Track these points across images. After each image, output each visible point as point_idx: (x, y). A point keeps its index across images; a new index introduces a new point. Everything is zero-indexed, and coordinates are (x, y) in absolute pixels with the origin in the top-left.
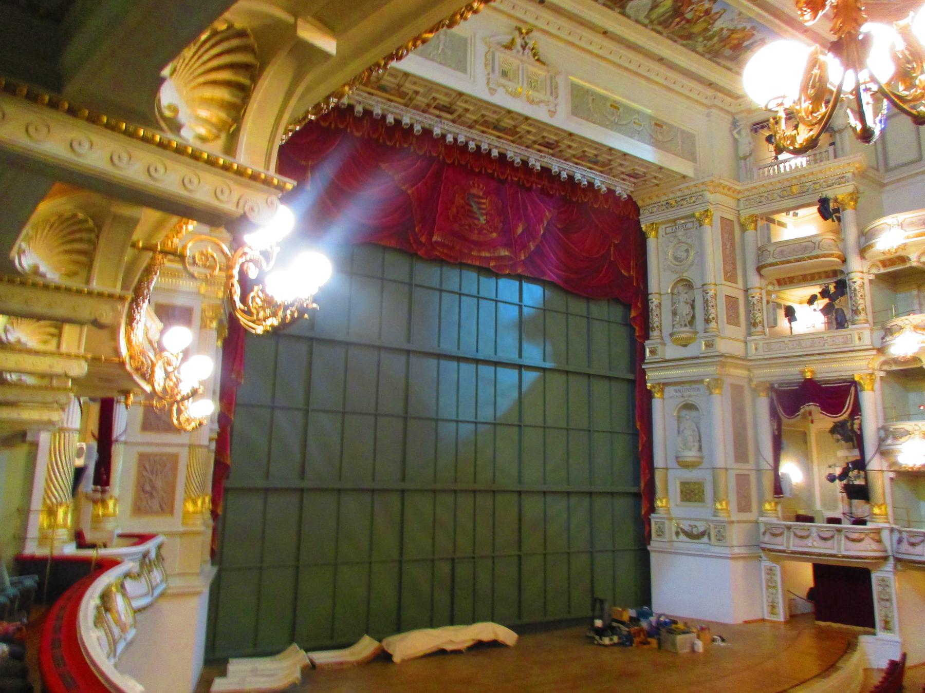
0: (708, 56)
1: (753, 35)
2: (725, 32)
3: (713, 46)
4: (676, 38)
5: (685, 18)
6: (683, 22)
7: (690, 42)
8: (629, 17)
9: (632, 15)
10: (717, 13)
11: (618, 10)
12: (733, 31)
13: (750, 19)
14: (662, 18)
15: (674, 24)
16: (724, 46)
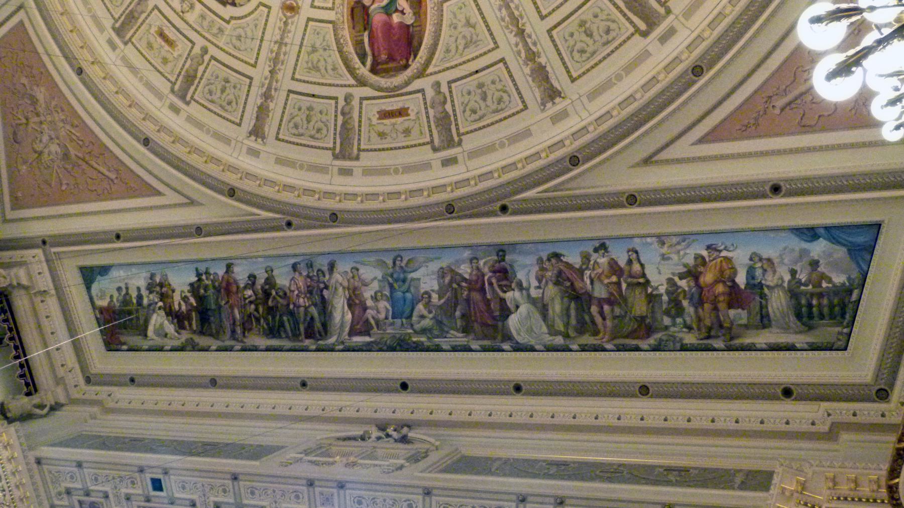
0: (718, 343)
1: (728, 260)
2: (683, 283)
3: (700, 320)
4: (634, 342)
5: (600, 302)
6: (606, 308)
7: (658, 336)
8: (532, 349)
9: (533, 342)
10: (630, 262)
11: (506, 346)
12: (692, 274)
13: (685, 237)
14: (573, 321)
15: (598, 319)
16: (716, 309)
